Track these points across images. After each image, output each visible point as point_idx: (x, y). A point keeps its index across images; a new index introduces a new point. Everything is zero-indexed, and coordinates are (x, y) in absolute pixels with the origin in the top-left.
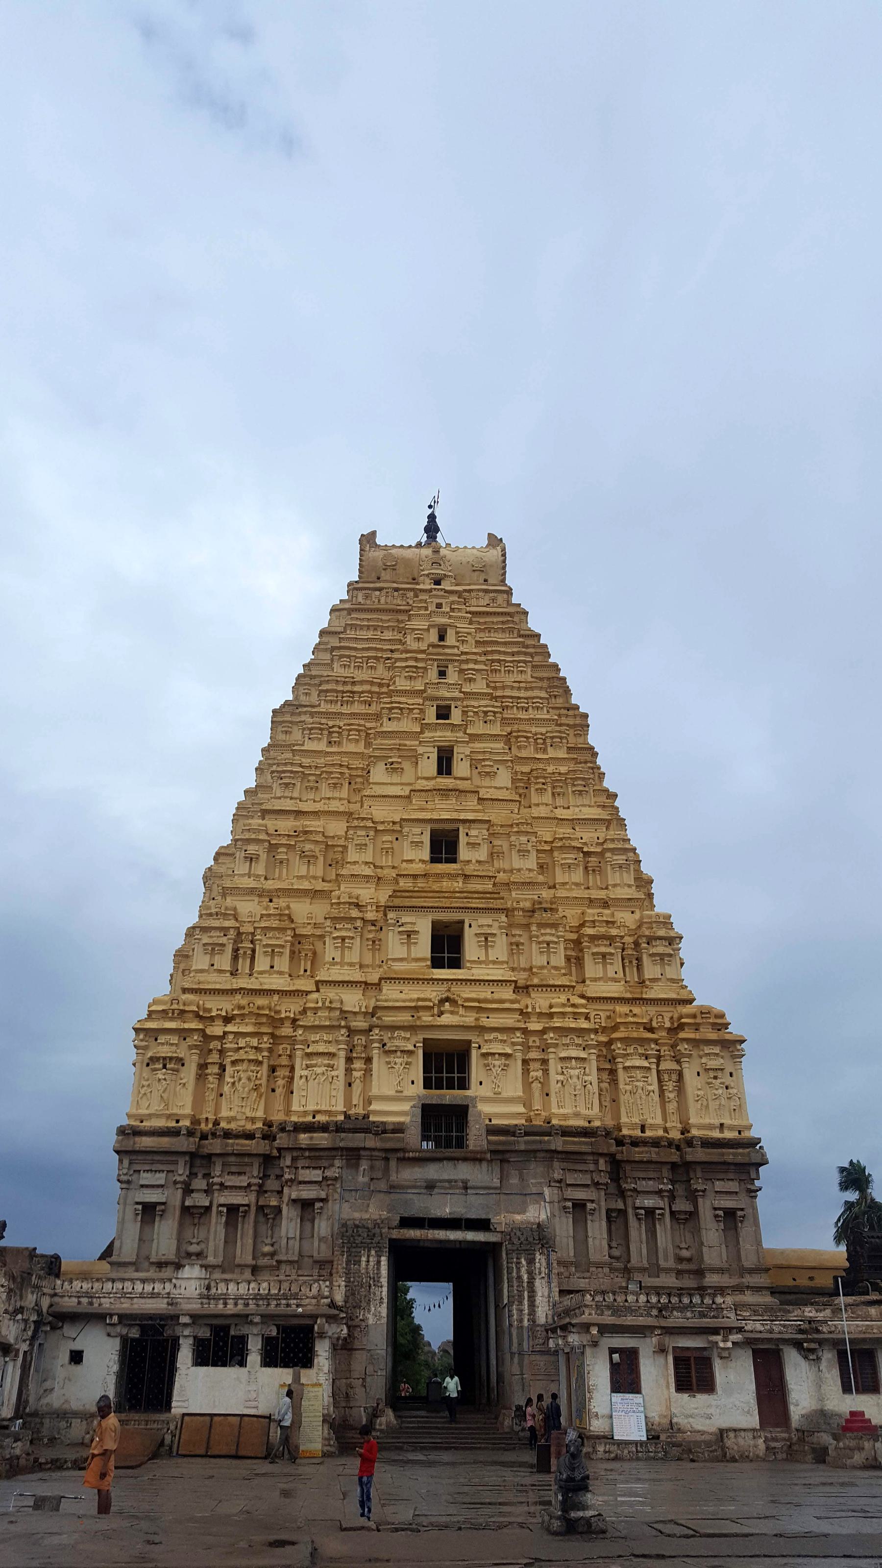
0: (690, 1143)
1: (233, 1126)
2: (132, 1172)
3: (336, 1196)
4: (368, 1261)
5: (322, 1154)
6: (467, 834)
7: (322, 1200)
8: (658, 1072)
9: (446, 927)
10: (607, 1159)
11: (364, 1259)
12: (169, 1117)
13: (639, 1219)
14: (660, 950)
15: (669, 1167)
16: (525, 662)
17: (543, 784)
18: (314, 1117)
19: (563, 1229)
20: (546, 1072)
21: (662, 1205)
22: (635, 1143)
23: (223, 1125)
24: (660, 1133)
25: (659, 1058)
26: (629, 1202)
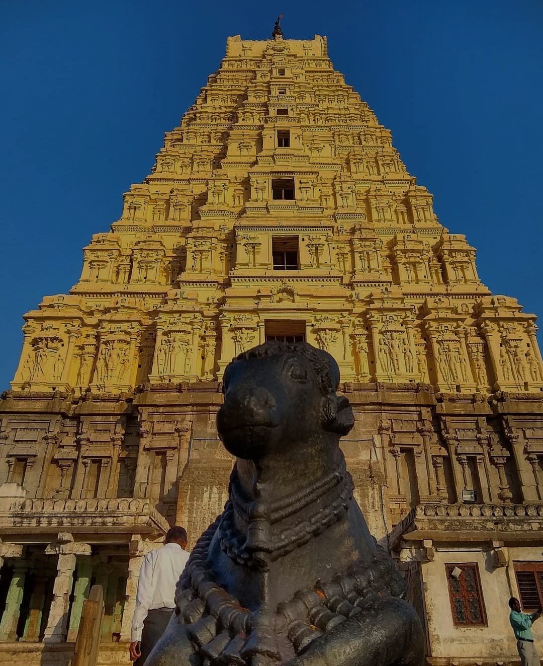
0: (502, 399)
1: (101, 392)
2: (8, 430)
3: (186, 445)
4: (210, 498)
5: (175, 409)
6: (300, 182)
7: (174, 448)
8: (467, 345)
9: (285, 243)
10: (429, 409)
11: (206, 495)
12: (45, 384)
13: (461, 464)
14: (459, 259)
15: (484, 418)
16: (343, 95)
17: (360, 160)
18: (170, 380)
19: (394, 469)
20: (371, 344)
21: (480, 450)
22: (452, 400)
23: (94, 391)
24: (474, 391)
25: (466, 334)
26: (453, 450)
